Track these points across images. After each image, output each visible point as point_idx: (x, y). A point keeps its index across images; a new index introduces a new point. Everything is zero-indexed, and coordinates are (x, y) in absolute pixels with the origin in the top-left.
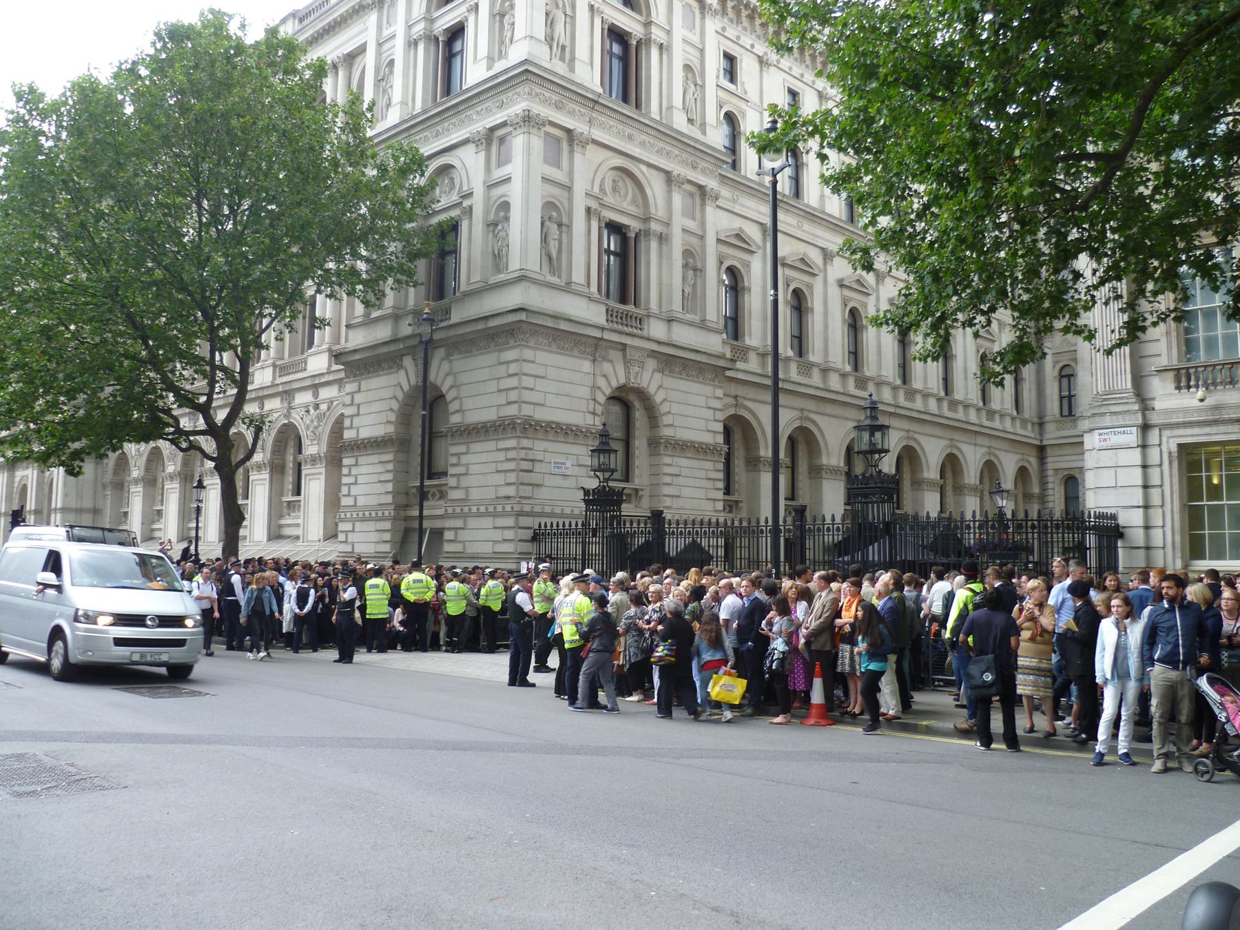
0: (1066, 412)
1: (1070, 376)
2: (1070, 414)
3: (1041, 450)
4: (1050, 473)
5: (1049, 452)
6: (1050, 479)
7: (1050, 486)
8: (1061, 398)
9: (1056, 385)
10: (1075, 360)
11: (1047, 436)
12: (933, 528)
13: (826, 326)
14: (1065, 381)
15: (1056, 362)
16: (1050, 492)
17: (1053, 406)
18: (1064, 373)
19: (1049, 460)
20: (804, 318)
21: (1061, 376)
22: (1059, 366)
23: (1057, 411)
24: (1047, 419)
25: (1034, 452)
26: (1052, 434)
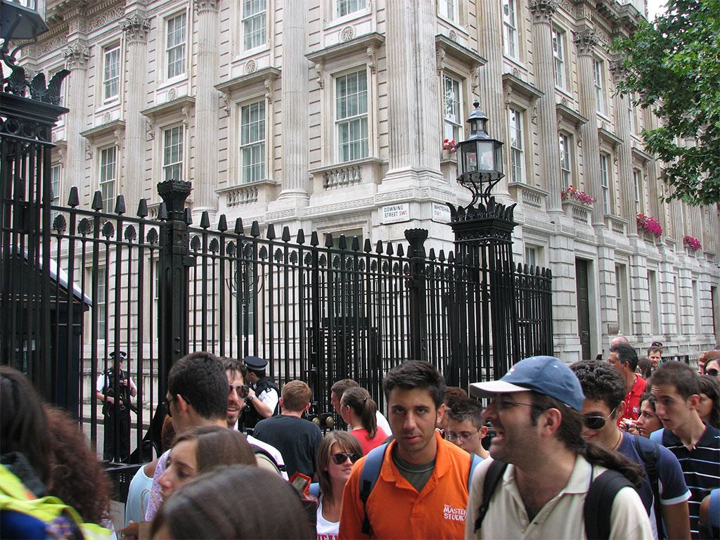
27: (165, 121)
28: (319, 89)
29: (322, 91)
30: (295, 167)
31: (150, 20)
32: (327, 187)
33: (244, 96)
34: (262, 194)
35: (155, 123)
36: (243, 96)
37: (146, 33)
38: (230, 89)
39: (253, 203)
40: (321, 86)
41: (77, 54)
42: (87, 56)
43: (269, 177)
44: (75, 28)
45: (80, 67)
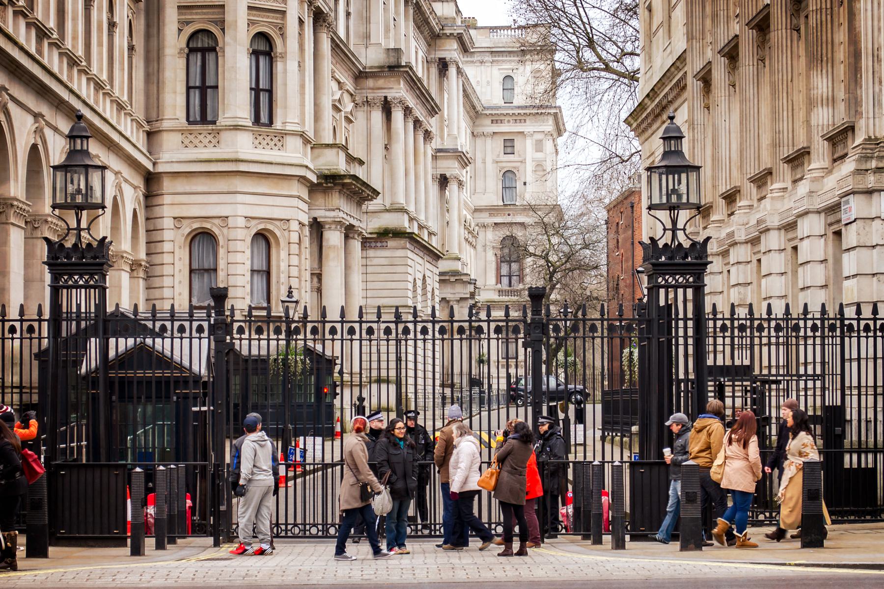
1: (204, 51)
3: (151, 181)
4: (167, 223)
5: (167, 185)
6: (167, 235)
7: (167, 247)
8: (189, 88)
9: (182, 62)
10: (221, 24)
11: (165, 156)
12: (78, 320)
15: (183, 23)
16: (167, 259)
17: (175, 102)
19: (167, 199)
21: (192, 50)
22: (189, 30)
23: (181, 114)
24: (166, 125)
25: (139, 182)
26: (174, 153)
32: (835, 161)
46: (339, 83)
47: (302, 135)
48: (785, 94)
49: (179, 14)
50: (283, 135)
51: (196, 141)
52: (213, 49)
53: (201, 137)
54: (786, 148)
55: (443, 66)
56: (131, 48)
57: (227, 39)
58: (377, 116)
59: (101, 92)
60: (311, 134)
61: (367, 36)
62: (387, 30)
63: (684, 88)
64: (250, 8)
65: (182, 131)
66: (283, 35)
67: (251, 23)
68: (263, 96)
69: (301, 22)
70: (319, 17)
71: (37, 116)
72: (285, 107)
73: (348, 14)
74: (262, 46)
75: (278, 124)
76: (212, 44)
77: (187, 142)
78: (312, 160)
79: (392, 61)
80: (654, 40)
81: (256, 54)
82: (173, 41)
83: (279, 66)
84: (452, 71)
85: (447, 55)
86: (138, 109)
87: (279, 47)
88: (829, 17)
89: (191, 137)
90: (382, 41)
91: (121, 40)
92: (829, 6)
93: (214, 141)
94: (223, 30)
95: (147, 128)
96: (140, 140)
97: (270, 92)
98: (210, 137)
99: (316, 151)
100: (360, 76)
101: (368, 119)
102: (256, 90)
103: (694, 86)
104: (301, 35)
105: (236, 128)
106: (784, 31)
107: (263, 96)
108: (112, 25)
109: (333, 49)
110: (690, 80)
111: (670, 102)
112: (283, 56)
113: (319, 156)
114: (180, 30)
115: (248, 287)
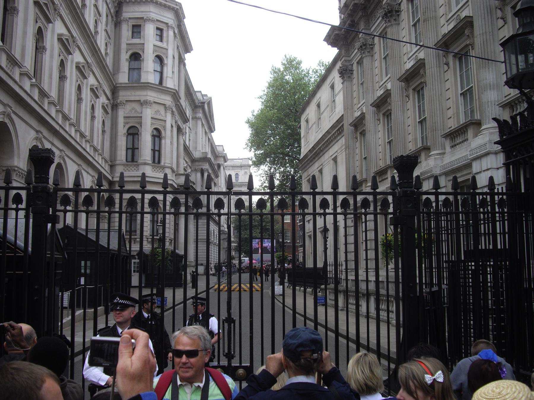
0: (130, 159)
2: (133, 160)
8: (127, 149)
10: (141, 124)
13: (25, 33)
14: (131, 137)
15: (126, 123)
17: (122, 154)
18: (131, 131)
20: (9, 17)
22: (128, 126)
23: (124, 158)
24: (117, 162)
27: (416, 82)
28: (504, 26)
29: (506, 26)
30: (490, 103)
31: (400, 4)
33: (458, 46)
34: (470, 133)
35: (408, 87)
36: (456, 48)
37: (398, 15)
38: (445, 44)
39: (465, 143)
40: (504, 21)
41: (364, 45)
42: (372, 45)
43: (477, 117)
44: (362, 26)
45: (369, 54)
46: (186, 161)
47: (172, 168)
48: (438, 102)
49: (124, 120)
50: (164, 167)
51: (129, 169)
52: (137, 134)
53: (131, 167)
54: (439, 131)
55: (219, 166)
56: (104, 132)
57: (143, 129)
58: (199, 175)
59: (97, 153)
60: (175, 169)
61: (196, 148)
62: (202, 147)
63: (343, 131)
64: (152, 118)
65: (124, 165)
66: (165, 130)
67: (152, 124)
68: (157, 153)
69: (172, 126)
70: (179, 130)
71: (37, 132)
72: (165, 157)
73: (190, 140)
74: (155, 133)
75: (162, 163)
76: (137, 132)
77: (126, 169)
78: (176, 180)
79: (204, 156)
80: (310, 131)
81: (154, 136)
82: (122, 130)
83: (163, 141)
84: (222, 168)
85: (220, 163)
86: (107, 155)
87: (163, 134)
88: (491, 37)
89: (128, 167)
90: (201, 149)
91: (98, 124)
92: (490, 31)
93: (136, 169)
94: (141, 126)
95: (110, 163)
96: (107, 168)
97: (159, 151)
98: (135, 167)
99: (177, 177)
100: (194, 161)
101: (196, 176)
102: (154, 150)
103: (348, 129)
104: (172, 131)
105: (145, 164)
106: (435, 68)
107: (157, 153)
108: (93, 117)
109: (184, 149)
110: (346, 127)
111: (322, 151)
112: (165, 138)
113: (178, 178)
114: (124, 126)
115: (149, 227)
